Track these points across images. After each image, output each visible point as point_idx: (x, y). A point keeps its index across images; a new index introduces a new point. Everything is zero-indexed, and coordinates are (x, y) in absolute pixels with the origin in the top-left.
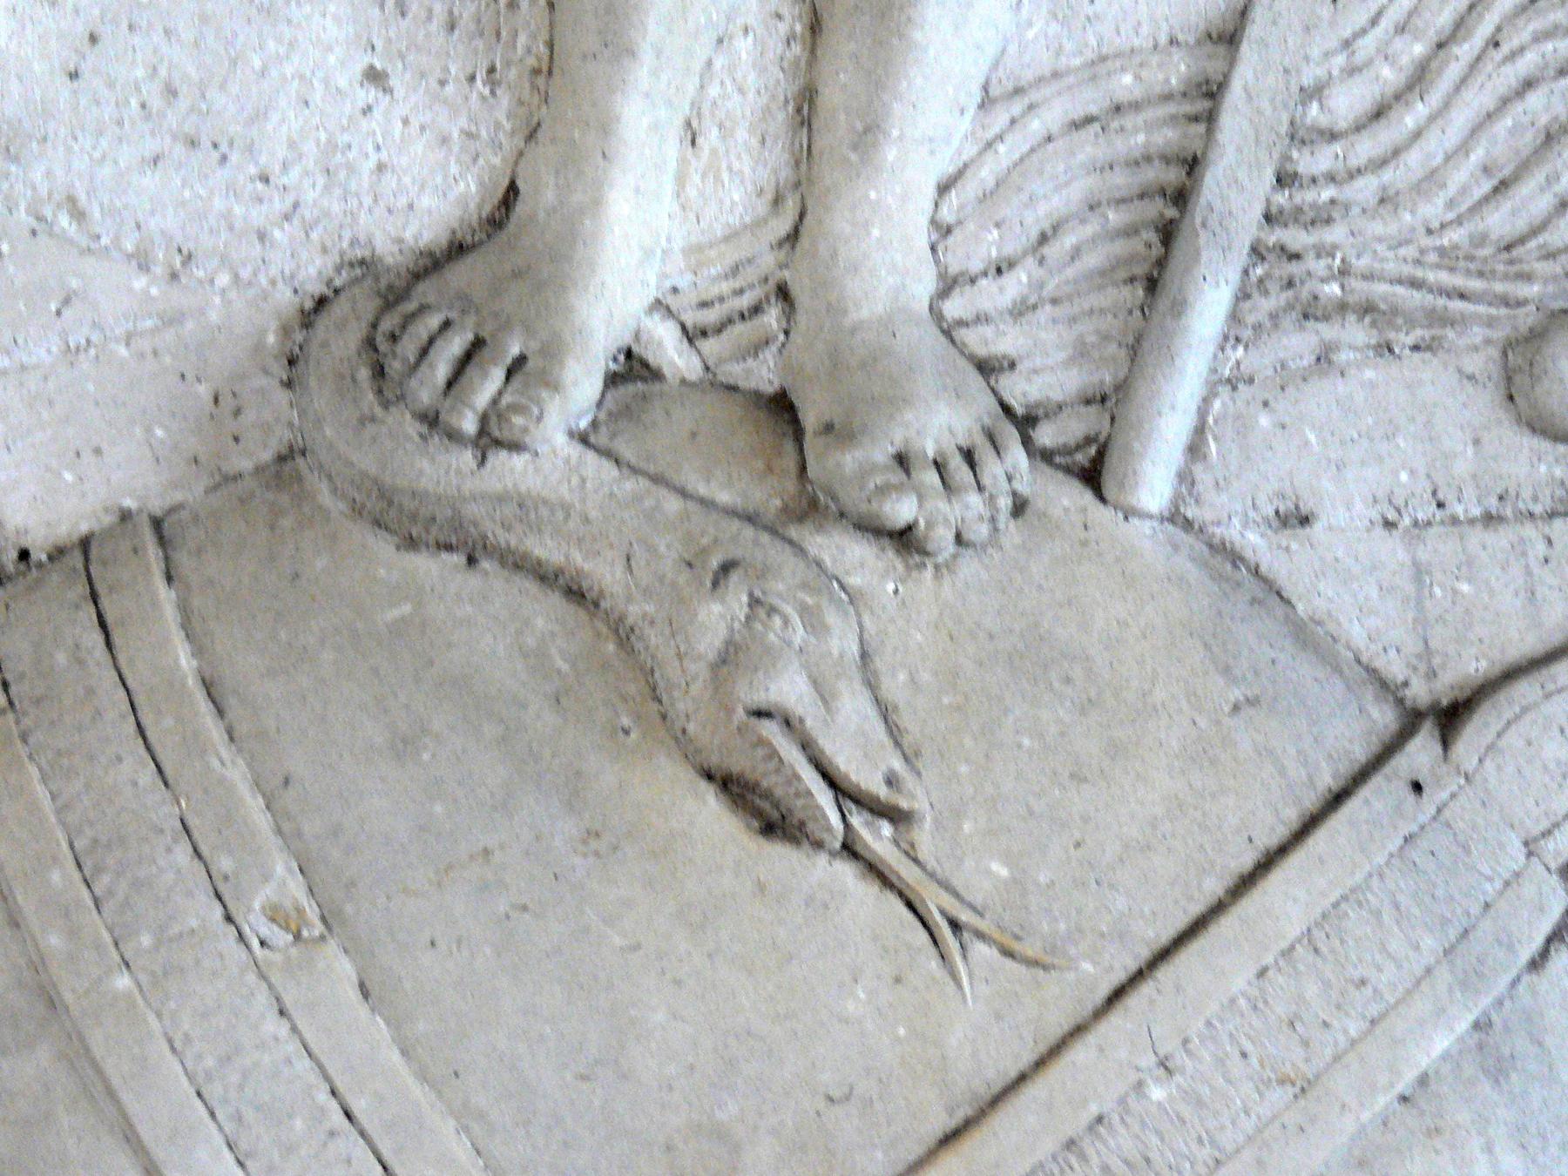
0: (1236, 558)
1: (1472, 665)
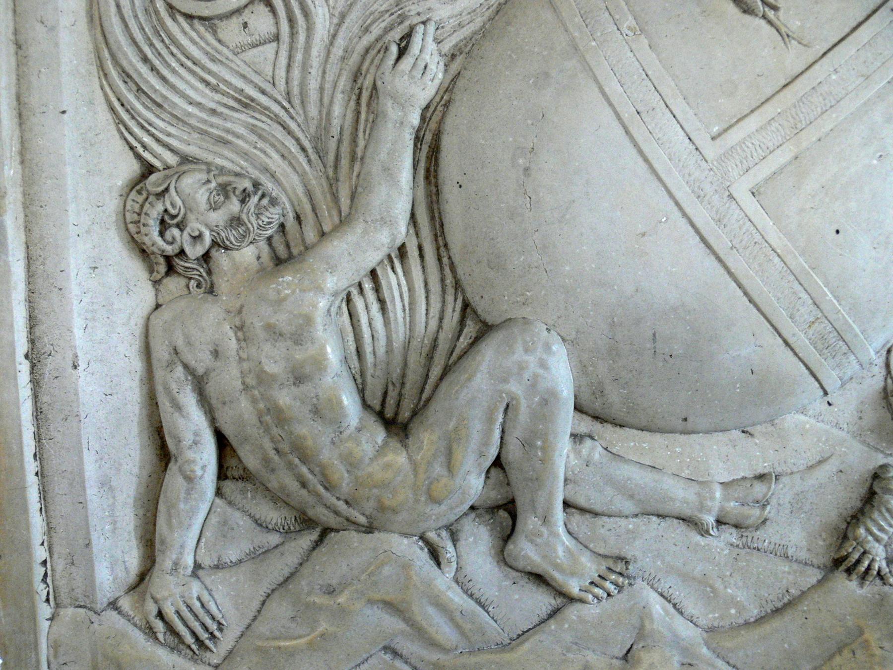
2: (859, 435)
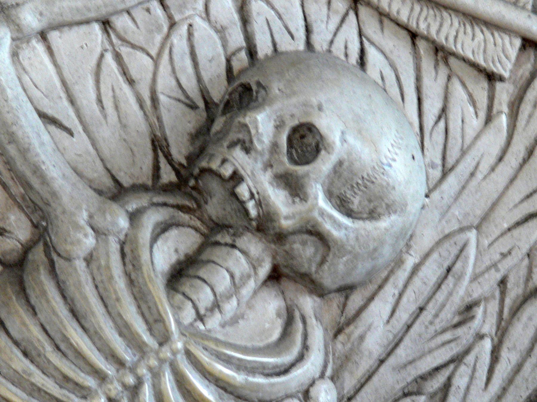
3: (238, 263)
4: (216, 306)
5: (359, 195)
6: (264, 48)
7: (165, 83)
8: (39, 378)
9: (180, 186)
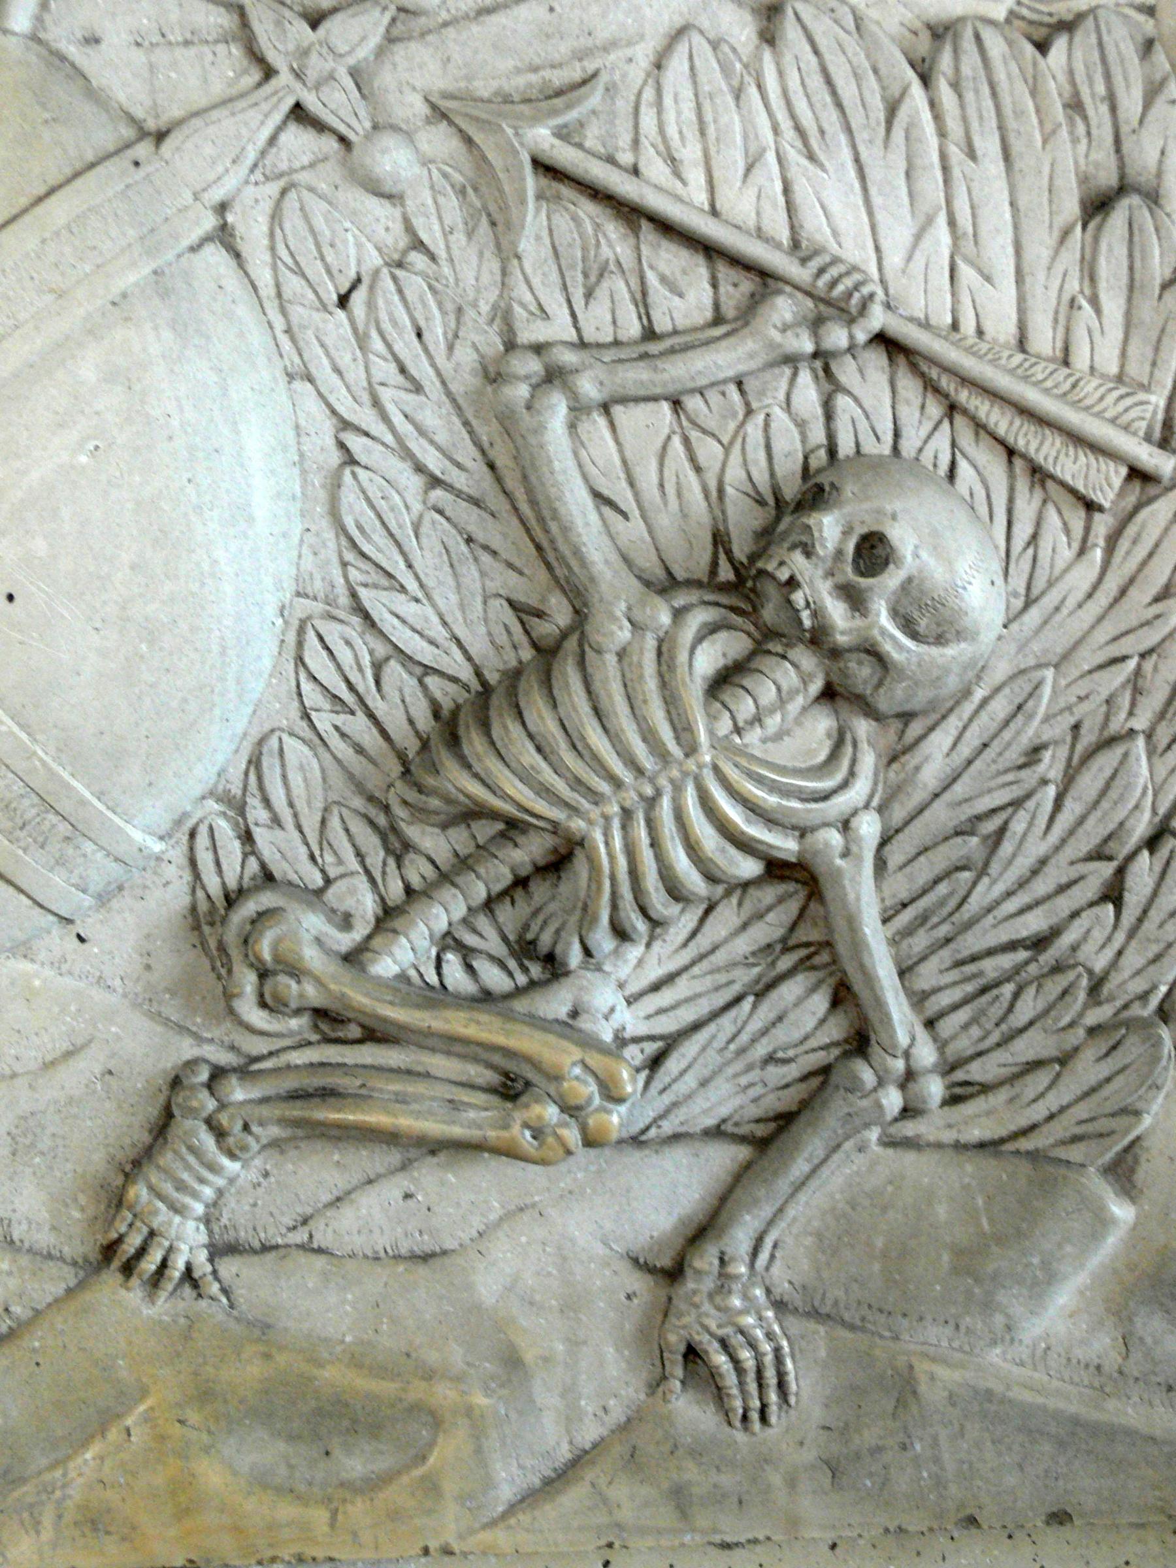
0: (63, 58)
1: (176, 112)
2: (147, 1004)
3: (787, 676)
4: (758, 719)
5: (926, 617)
6: (845, 447)
7: (735, 474)
8: (547, 775)
9: (736, 586)
